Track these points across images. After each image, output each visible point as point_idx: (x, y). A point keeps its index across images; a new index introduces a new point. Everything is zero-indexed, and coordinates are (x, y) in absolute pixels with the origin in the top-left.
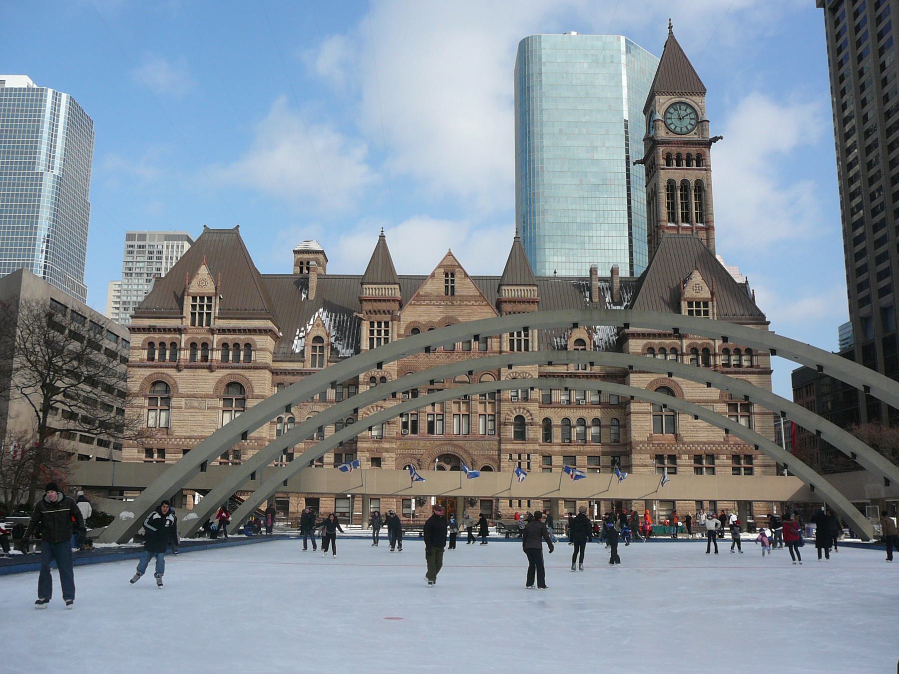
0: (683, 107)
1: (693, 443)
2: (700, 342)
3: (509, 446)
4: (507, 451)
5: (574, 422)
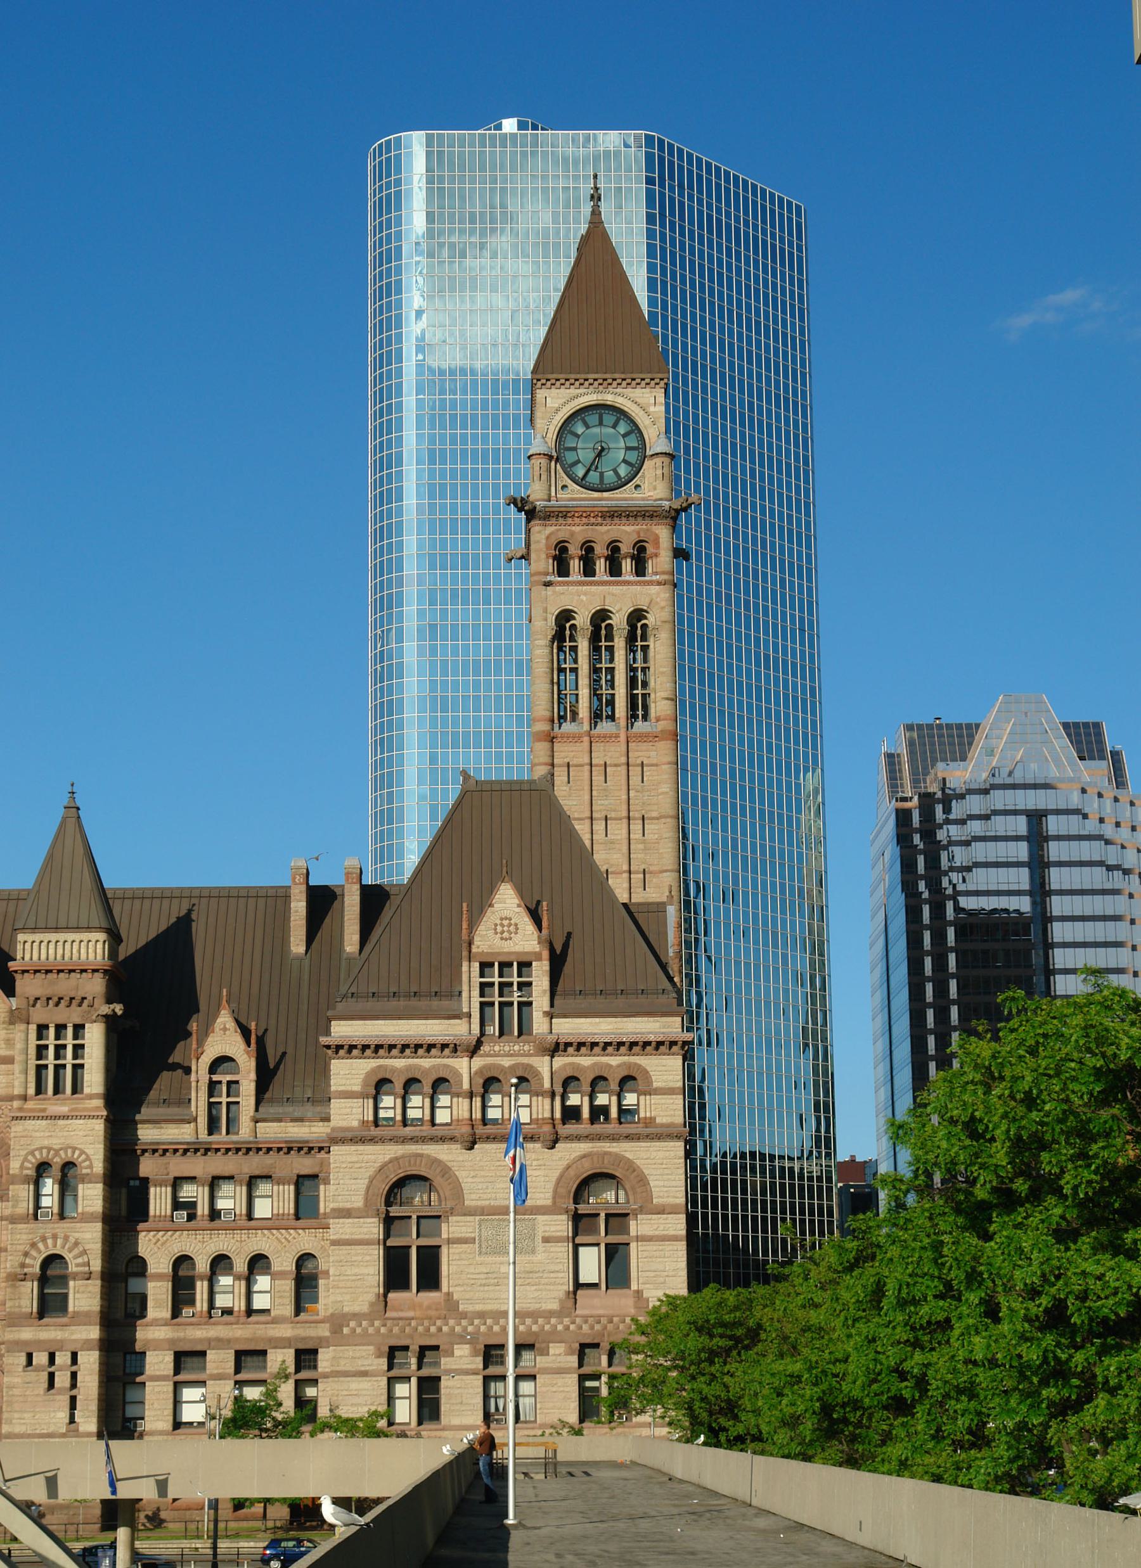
0: (609, 419)
1: (482, 1315)
2: (506, 1062)
3: (27, 1334)
4: (16, 1345)
5: (202, 1265)
